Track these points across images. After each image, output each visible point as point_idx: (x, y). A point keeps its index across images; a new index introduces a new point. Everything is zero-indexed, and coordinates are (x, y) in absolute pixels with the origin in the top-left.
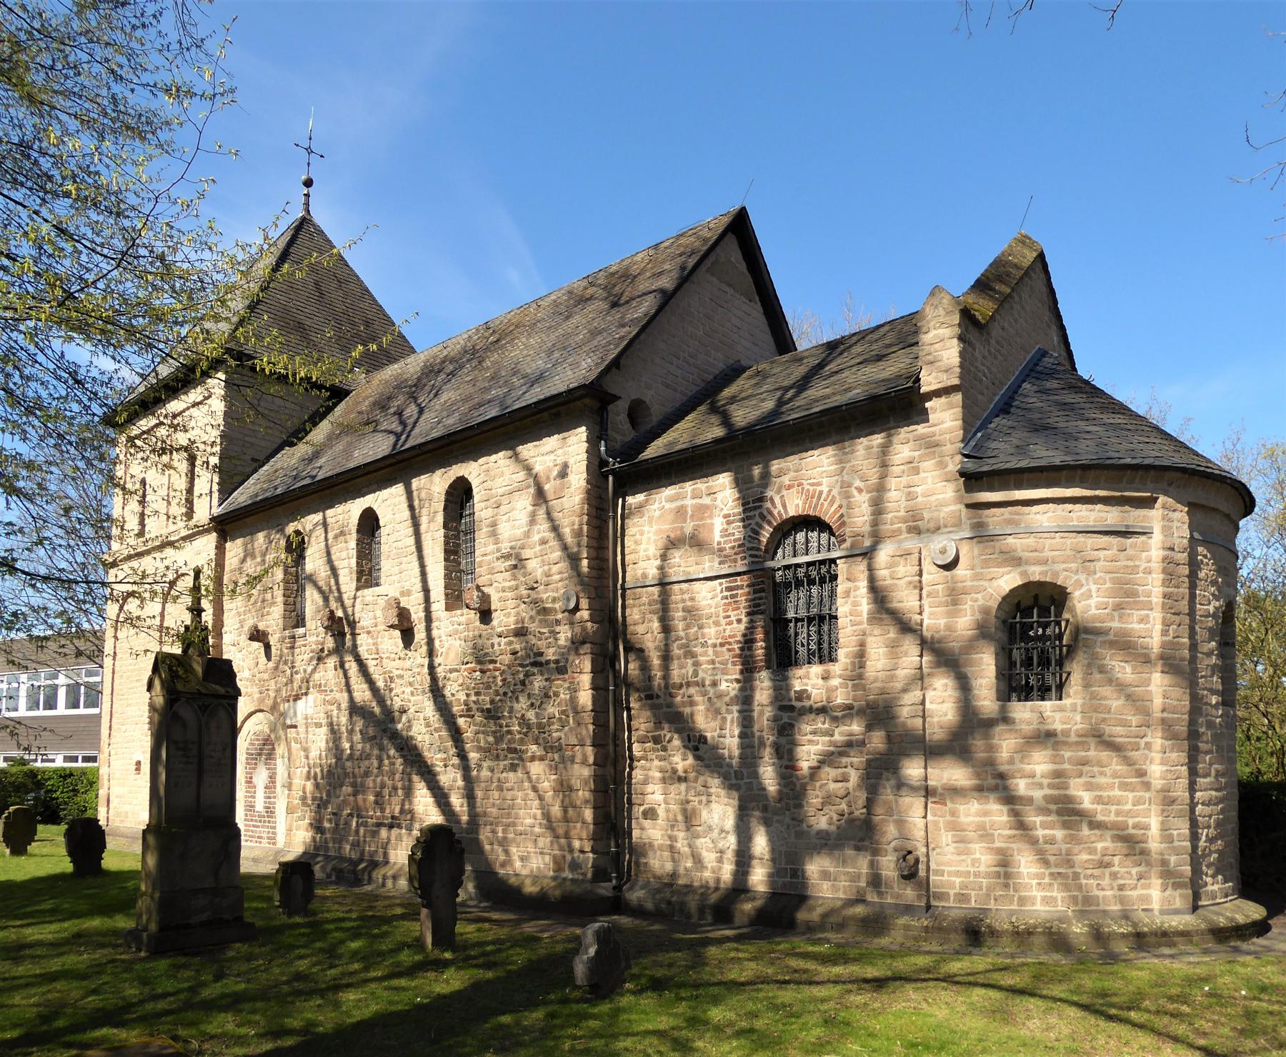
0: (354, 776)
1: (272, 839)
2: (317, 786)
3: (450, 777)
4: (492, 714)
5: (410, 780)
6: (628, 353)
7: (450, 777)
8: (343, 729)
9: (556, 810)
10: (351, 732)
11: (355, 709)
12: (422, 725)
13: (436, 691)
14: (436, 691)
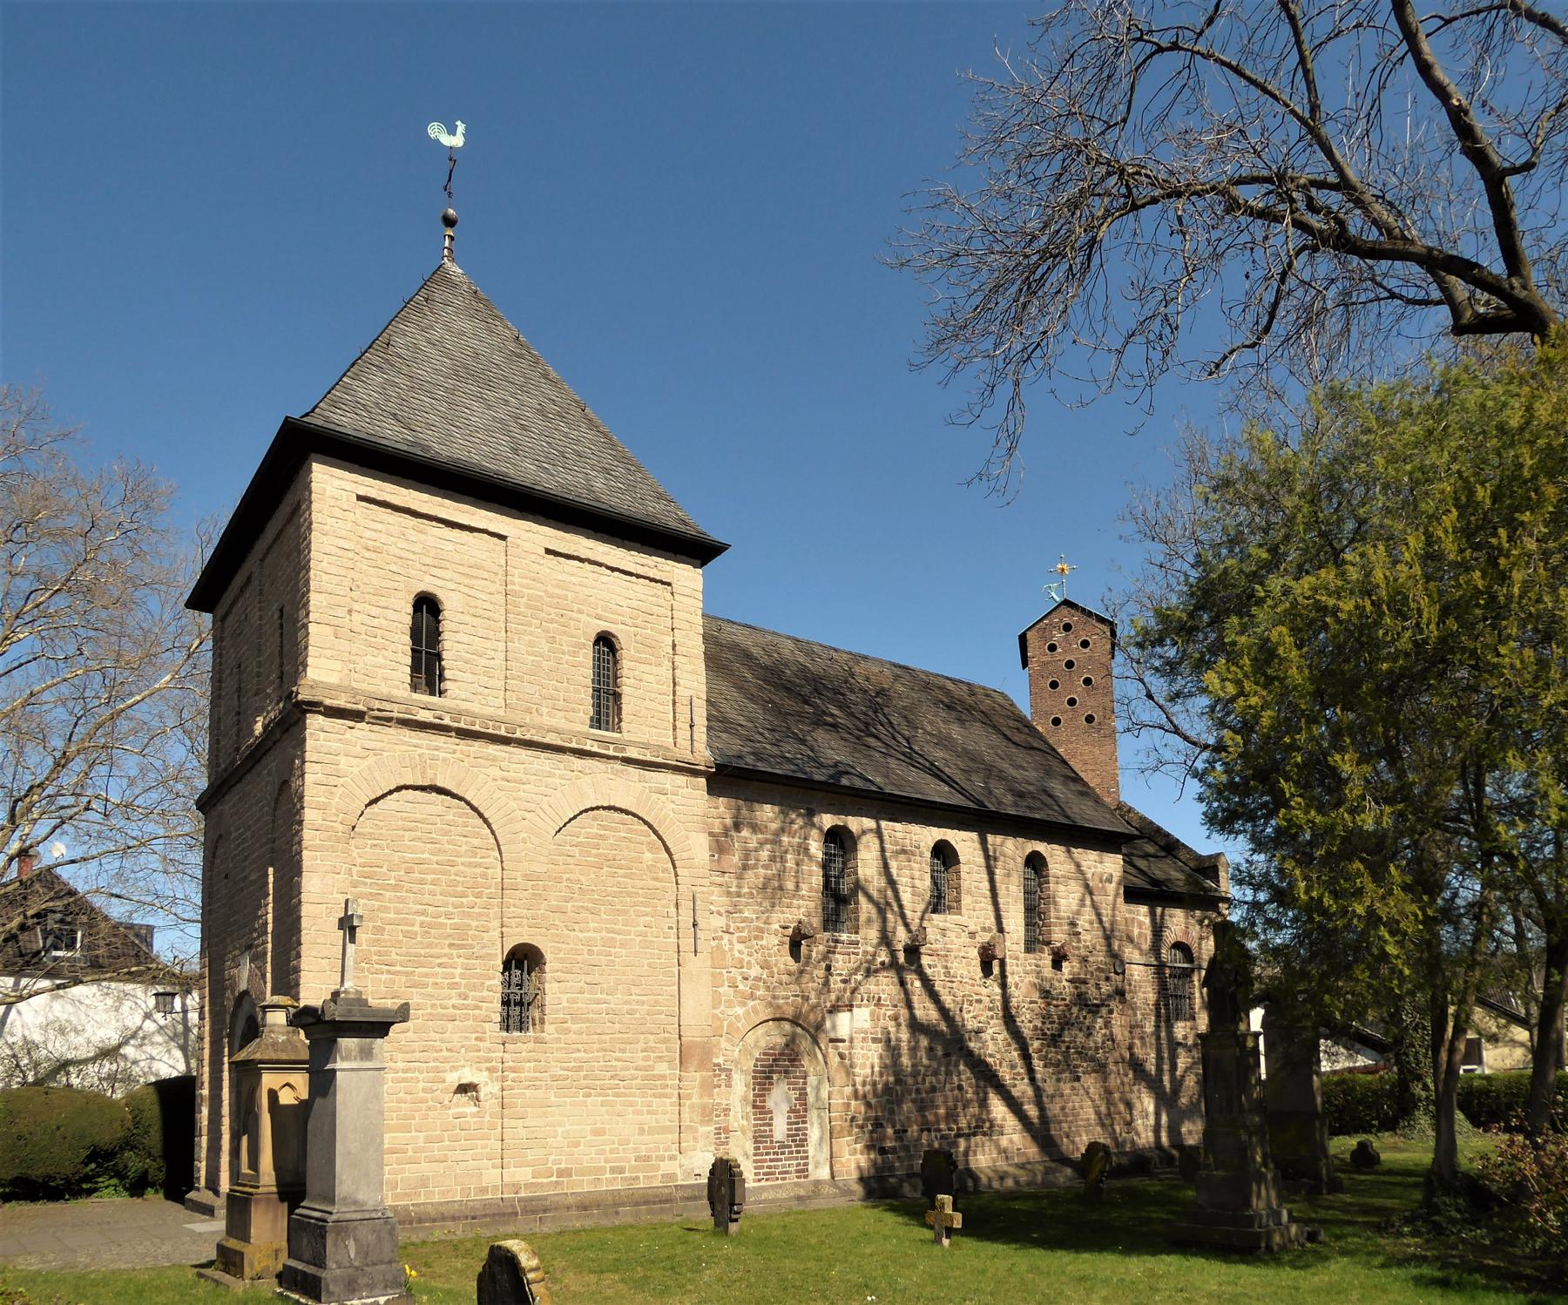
0: (918, 1091)
1: (803, 1172)
2: (868, 1105)
3: (1022, 1089)
4: (1054, 1040)
5: (986, 1093)
7: (1022, 1089)
8: (904, 1045)
9: (1103, 1109)
10: (914, 1050)
11: (916, 1026)
12: (994, 1045)
13: (1009, 1019)
14: (1009, 1019)
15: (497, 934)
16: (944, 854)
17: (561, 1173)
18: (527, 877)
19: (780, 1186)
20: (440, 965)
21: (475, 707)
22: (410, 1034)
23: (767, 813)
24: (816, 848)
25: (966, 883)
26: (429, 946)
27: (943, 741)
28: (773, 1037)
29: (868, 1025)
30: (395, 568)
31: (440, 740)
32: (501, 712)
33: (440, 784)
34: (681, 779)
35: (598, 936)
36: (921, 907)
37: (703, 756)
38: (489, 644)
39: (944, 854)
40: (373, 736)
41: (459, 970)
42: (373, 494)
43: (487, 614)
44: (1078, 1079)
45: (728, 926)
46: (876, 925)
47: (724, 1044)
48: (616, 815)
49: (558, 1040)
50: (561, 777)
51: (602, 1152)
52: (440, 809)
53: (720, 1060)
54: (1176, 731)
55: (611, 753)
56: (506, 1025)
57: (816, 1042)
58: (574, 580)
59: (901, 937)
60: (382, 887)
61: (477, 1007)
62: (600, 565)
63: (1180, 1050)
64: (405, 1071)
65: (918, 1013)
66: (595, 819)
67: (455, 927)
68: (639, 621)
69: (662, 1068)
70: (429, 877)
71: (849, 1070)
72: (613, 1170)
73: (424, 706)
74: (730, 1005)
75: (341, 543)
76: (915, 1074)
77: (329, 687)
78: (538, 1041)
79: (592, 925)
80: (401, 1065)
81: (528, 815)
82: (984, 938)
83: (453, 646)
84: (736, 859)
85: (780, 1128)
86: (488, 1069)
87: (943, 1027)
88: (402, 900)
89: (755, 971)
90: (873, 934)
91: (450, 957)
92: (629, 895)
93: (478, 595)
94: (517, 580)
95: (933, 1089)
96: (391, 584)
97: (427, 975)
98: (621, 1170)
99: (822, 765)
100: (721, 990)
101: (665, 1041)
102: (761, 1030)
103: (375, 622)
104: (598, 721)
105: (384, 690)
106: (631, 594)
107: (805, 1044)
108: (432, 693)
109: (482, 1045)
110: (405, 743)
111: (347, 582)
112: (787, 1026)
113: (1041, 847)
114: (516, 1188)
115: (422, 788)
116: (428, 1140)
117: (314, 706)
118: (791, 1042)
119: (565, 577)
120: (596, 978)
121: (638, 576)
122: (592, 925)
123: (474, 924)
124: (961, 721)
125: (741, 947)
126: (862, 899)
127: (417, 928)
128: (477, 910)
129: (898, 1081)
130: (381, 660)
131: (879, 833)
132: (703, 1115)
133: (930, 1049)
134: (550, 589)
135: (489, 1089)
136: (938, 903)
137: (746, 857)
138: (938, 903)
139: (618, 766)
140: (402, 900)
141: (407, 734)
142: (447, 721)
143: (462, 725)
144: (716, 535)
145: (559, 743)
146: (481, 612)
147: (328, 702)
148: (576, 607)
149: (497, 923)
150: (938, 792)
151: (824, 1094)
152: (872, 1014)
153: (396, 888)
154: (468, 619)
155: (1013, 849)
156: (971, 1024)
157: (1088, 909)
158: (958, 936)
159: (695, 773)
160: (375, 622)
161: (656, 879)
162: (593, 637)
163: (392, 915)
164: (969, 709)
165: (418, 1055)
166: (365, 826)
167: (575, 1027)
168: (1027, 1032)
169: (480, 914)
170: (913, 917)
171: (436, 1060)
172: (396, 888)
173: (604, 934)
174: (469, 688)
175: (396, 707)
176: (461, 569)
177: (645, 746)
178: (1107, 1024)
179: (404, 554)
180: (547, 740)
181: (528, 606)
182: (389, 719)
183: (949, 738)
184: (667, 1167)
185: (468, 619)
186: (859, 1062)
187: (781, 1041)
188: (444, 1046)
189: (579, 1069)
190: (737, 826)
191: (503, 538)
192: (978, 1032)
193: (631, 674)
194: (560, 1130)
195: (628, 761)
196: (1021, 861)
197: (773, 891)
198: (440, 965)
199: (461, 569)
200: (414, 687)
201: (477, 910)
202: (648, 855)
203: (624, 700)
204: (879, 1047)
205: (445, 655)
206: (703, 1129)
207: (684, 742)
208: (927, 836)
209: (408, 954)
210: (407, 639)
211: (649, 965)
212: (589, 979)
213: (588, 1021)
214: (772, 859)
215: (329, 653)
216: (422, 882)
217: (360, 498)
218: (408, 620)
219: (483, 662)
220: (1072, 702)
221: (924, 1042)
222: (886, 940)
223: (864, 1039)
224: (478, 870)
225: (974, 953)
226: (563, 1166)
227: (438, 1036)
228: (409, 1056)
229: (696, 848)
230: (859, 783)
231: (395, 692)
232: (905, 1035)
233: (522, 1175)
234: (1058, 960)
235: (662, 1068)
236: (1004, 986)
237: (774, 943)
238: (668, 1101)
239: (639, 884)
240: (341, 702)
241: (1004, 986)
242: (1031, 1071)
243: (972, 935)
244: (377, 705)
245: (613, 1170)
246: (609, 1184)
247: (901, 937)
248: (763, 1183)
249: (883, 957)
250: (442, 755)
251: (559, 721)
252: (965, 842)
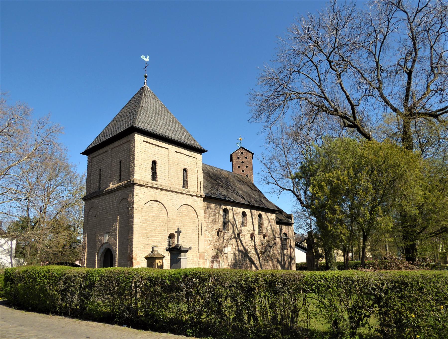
3: (258, 264)
4: (263, 253)
6: (117, 144)
8: (237, 254)
10: (239, 255)
11: (239, 251)
12: (253, 254)
14: (256, 249)
16: (244, 214)
18: (172, 219)
21: (163, 184)
23: (213, 205)
24: (222, 213)
25: (248, 220)
27: (241, 189)
28: (214, 253)
29: (230, 250)
33: (157, 200)
34: (199, 199)
36: (240, 225)
37: (203, 194)
38: (165, 171)
39: (244, 214)
44: (268, 262)
46: (232, 229)
52: (157, 205)
54: (278, 185)
57: (221, 254)
59: (237, 232)
63: (285, 256)
65: (239, 248)
71: (227, 260)
76: (239, 261)
77: (140, 180)
82: (252, 232)
84: (207, 215)
87: (244, 251)
89: (211, 239)
90: (231, 231)
95: (242, 264)
99: (222, 195)
102: (212, 251)
104: (183, 187)
107: (219, 254)
108: (154, 180)
112: (216, 250)
113: (261, 212)
115: (154, 201)
117: (136, 184)
118: (217, 254)
124: (243, 185)
125: (208, 233)
126: (230, 223)
129: (236, 262)
131: (232, 209)
133: (242, 255)
136: (243, 224)
137: (209, 215)
138: (243, 224)
139: (188, 196)
141: (152, 189)
142: (159, 187)
150: (243, 201)
151: (223, 265)
154: (161, 165)
155: (256, 213)
156: (249, 250)
157: (269, 226)
159: (201, 197)
164: (243, 181)
168: (259, 252)
170: (238, 227)
174: (161, 181)
177: (193, 192)
178: (273, 251)
183: (241, 189)
185: (161, 165)
186: (229, 258)
187: (215, 253)
190: (208, 208)
192: (250, 252)
195: (190, 195)
196: (257, 216)
197: (214, 222)
202: (193, 214)
203: (189, 182)
204: (232, 255)
205: (158, 173)
207: (199, 191)
208: (241, 210)
214: (214, 215)
217: (144, 141)
218: (151, 166)
220: (243, 171)
221: (241, 254)
222: (234, 232)
225: (249, 235)
229: (201, 212)
230: (229, 199)
232: (237, 253)
234: (264, 236)
236: (255, 242)
237: (214, 232)
240: (141, 183)
241: (255, 242)
242: (259, 260)
243: (249, 231)
244: (147, 184)
247: (237, 232)
249: (233, 236)
251: (177, 186)
252: (247, 211)
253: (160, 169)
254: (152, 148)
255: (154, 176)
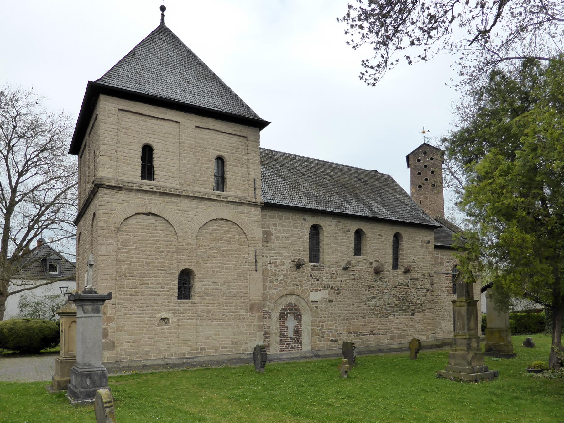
1: (300, 348)
15: (176, 265)
17: (202, 349)
18: (187, 245)
19: (291, 353)
20: (153, 277)
21: (167, 185)
22: (142, 301)
26: (149, 270)
30: (134, 135)
31: (153, 197)
32: (177, 186)
33: (153, 212)
34: (250, 208)
35: (217, 265)
40: (126, 196)
41: (161, 278)
42: (125, 108)
43: (172, 151)
45: (270, 261)
47: (268, 303)
48: (224, 222)
49: (201, 303)
50: (202, 208)
51: (218, 342)
53: (267, 309)
55: (222, 199)
56: (180, 297)
58: (207, 137)
60: (131, 249)
61: (168, 291)
62: (218, 131)
64: (139, 314)
66: (215, 223)
67: (159, 263)
68: (234, 151)
69: (243, 312)
70: (149, 246)
72: (222, 348)
73: (146, 184)
74: (270, 289)
75: (113, 127)
78: (192, 303)
79: (214, 262)
80: (138, 312)
81: (188, 223)
83: (157, 163)
85: (291, 334)
86: (173, 313)
88: (138, 254)
91: (158, 274)
92: (229, 250)
93: (168, 144)
94: (184, 138)
96: (133, 141)
97: (148, 280)
98: (226, 348)
100: (267, 284)
101: (243, 302)
103: (127, 155)
105: (131, 179)
106: (231, 141)
109: (170, 304)
110: (139, 198)
111: (115, 141)
114: (184, 354)
116: (149, 338)
119: (204, 136)
120: (216, 281)
121: (233, 135)
122: (214, 262)
123: (167, 262)
127: (144, 264)
128: (168, 257)
130: (129, 168)
132: (259, 328)
134: (197, 141)
135: (173, 320)
140: (138, 254)
141: (140, 195)
142: (155, 189)
143: (161, 191)
144: (265, 118)
145: (201, 196)
146: (169, 150)
147: (107, 184)
148: (208, 147)
149: (176, 261)
152: (329, 292)
153: (135, 250)
158: (365, 264)
160: (127, 155)
161: (239, 245)
162: (215, 157)
163: (134, 259)
165: (145, 308)
166: (124, 229)
167: (208, 298)
169: (169, 258)
171: (152, 310)
172: (135, 250)
173: (219, 264)
174: (163, 177)
175: (135, 185)
176: (161, 135)
179: (137, 130)
180: (195, 195)
181: (188, 147)
182: (132, 189)
184: (244, 347)
188: (155, 305)
189: (209, 312)
191: (179, 122)
193: (230, 170)
194: (201, 334)
198: (153, 277)
199: (161, 135)
200: (143, 177)
201: (168, 257)
202: (237, 236)
205: (155, 166)
206: (258, 333)
209: (141, 273)
210: (140, 160)
211: (237, 276)
212: (213, 281)
213: (213, 296)
215: (108, 166)
216: (146, 247)
218: (140, 154)
219: (171, 168)
223: (325, 301)
224: (168, 243)
225: (372, 269)
226: (203, 346)
227: (153, 302)
228: (142, 309)
231: (135, 180)
233: (187, 350)
235: (243, 312)
238: (245, 324)
239: (233, 246)
240: (113, 184)
243: (371, 263)
244: (127, 184)
245: (222, 348)
246: (222, 354)
248: (283, 352)
250: (153, 202)
253: (160, 159)
254: (141, 123)
255: (148, 171)
